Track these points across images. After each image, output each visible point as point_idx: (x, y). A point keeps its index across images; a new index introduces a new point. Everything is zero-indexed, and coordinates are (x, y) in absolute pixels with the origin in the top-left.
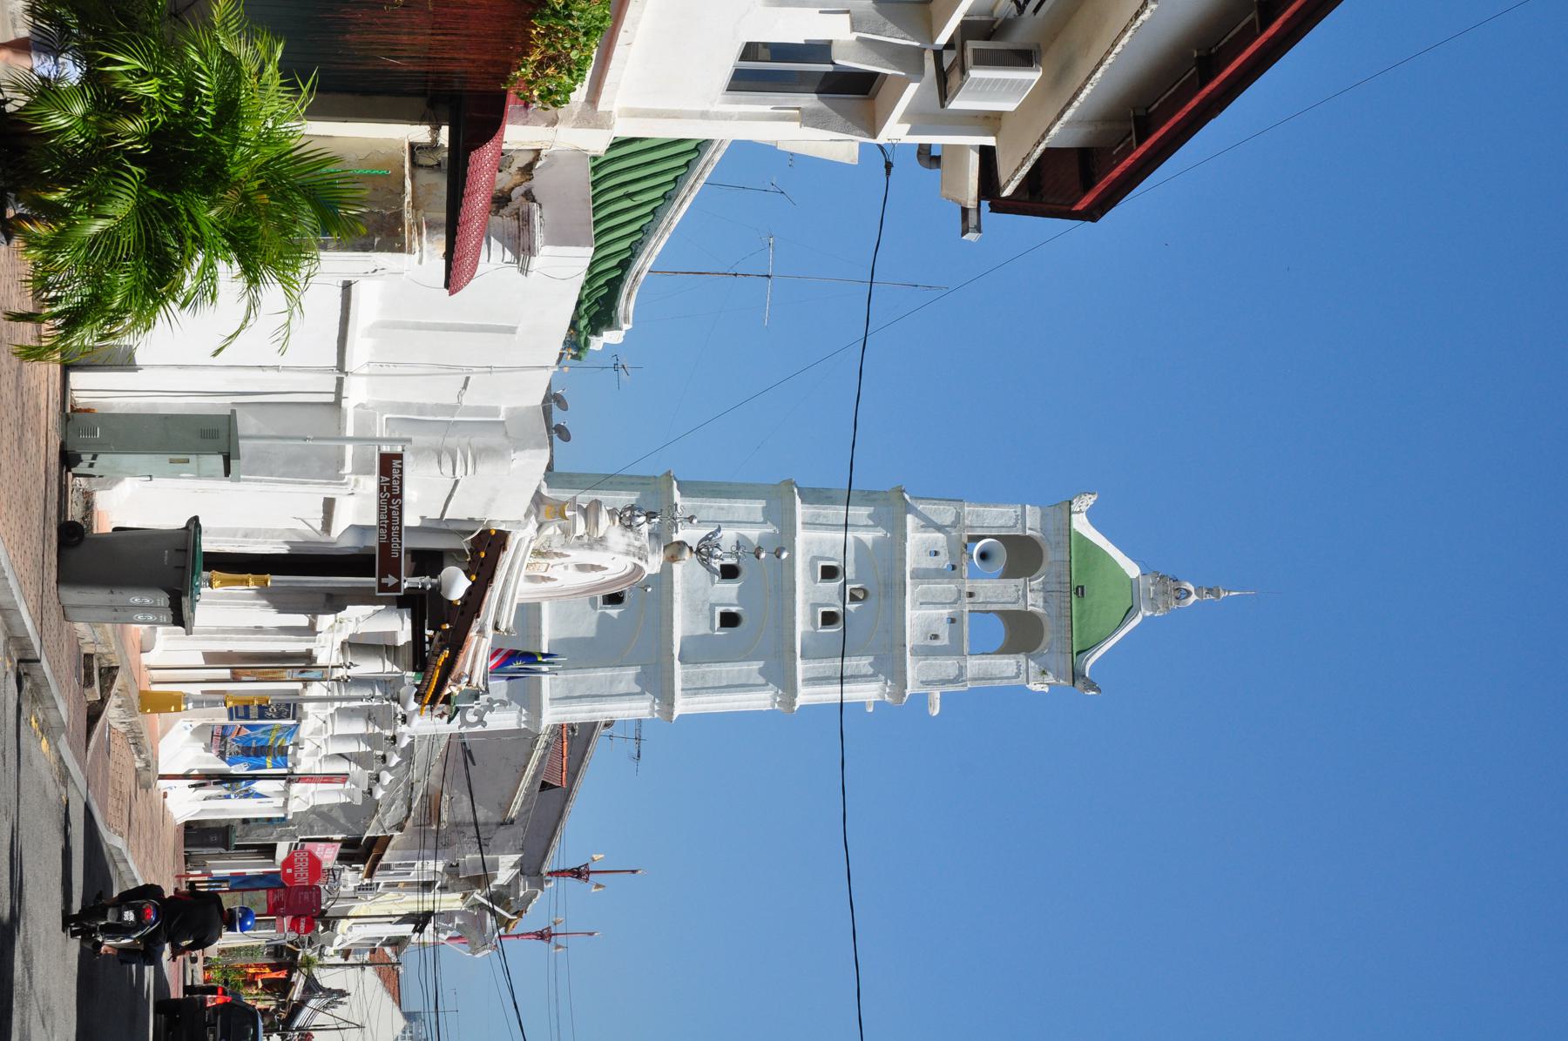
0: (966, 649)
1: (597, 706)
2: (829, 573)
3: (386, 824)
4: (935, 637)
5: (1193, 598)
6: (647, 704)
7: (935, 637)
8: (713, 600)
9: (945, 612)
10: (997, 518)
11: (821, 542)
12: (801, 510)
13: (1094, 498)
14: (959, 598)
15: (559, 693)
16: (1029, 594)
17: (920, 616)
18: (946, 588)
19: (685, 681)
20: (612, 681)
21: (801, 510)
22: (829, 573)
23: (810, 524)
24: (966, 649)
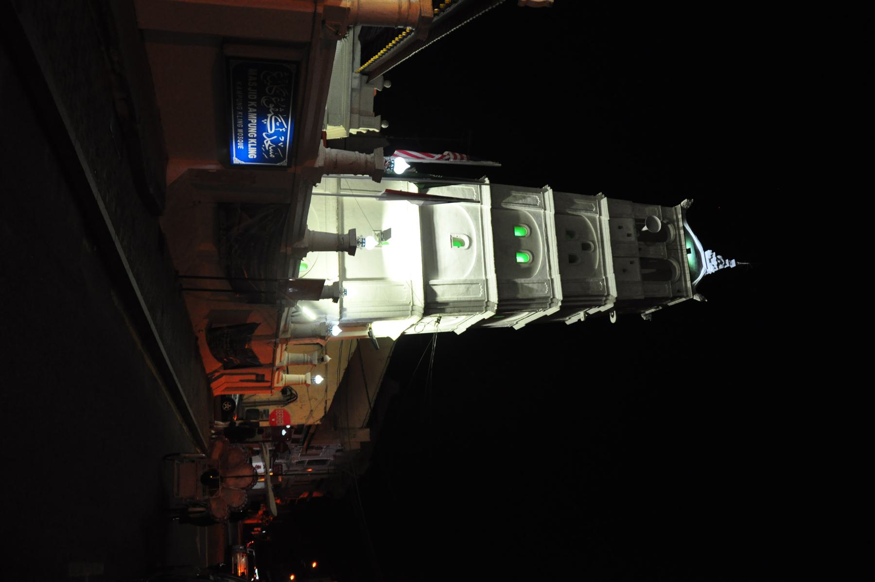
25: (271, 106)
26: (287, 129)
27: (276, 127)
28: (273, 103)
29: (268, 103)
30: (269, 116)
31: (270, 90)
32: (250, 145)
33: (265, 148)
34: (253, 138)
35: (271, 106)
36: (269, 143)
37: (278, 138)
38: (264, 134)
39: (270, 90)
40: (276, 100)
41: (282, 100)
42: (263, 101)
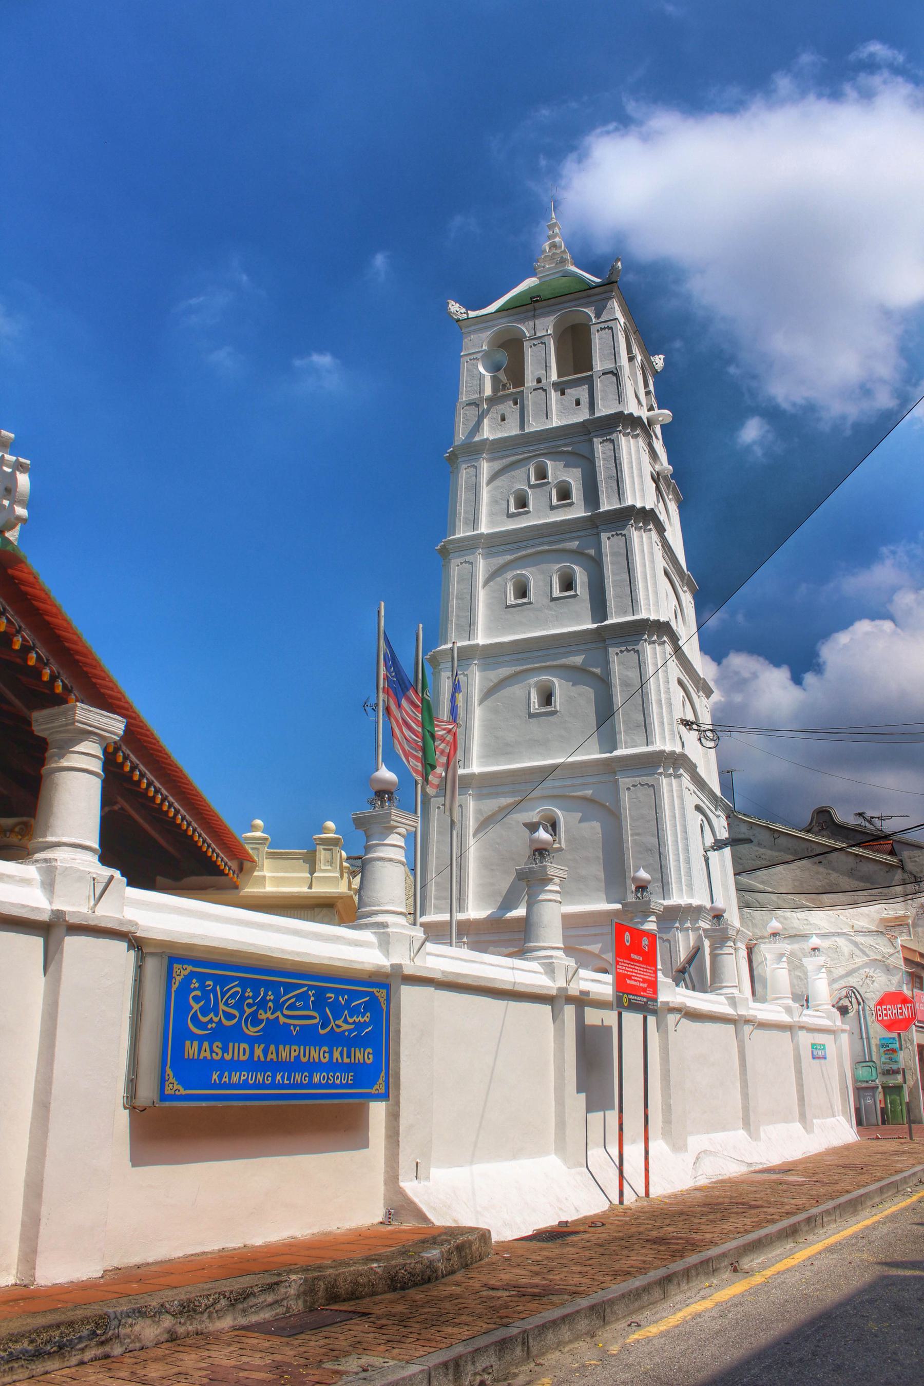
0: (590, 373)
1: (653, 697)
2: (522, 503)
3: (892, 951)
4: (578, 403)
5: (557, 239)
6: (649, 648)
7: (578, 403)
8: (546, 601)
9: (554, 395)
10: (477, 377)
11: (491, 514)
12: (462, 532)
13: (452, 302)
14: (542, 388)
15: (642, 738)
16: (539, 335)
17: (559, 414)
18: (531, 400)
19: (625, 613)
20: (625, 684)
21: (462, 532)
22: (522, 503)
23: (474, 522)
24: (590, 373)
25: (262, 1015)
26: (311, 987)
27: (305, 1007)
28: (256, 1012)
29: (256, 1021)
30: (282, 1020)
31: (229, 1016)
32: (346, 1060)
33: (350, 1031)
34: (331, 1053)
35: (262, 1015)
36: (339, 1022)
37: (330, 1005)
38: (322, 1032)
39: (229, 1016)
40: (249, 1006)
41: (249, 993)
42: (251, 1031)
